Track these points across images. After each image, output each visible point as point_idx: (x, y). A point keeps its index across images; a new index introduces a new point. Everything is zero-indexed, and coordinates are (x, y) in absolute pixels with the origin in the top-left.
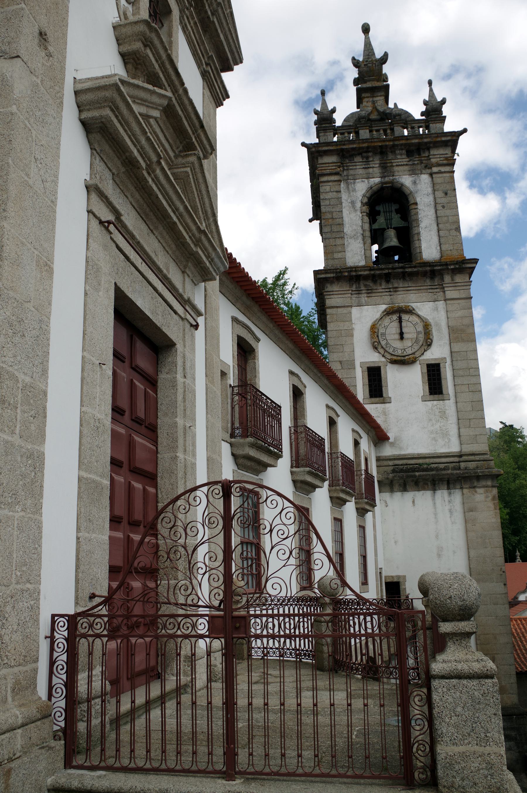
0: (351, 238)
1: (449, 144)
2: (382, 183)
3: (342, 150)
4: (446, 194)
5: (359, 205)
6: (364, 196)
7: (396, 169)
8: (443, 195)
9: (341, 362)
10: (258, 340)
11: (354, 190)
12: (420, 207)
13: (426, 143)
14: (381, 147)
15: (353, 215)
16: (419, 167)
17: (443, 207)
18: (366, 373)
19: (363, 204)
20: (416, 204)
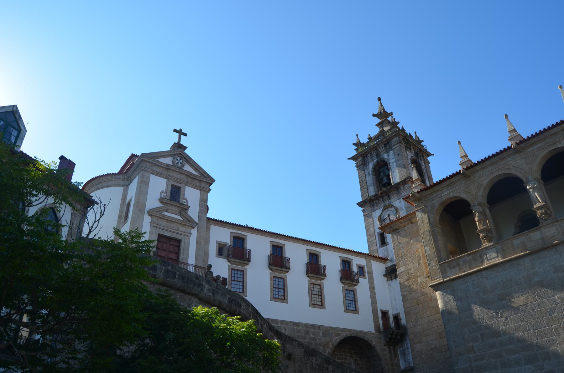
0: (369, 186)
1: (397, 135)
2: (377, 161)
3: (362, 155)
4: (399, 155)
5: (371, 172)
6: (372, 168)
7: (382, 153)
8: (398, 156)
9: (370, 235)
10: (247, 236)
11: (369, 168)
12: (390, 164)
13: (389, 139)
14: (374, 147)
15: (369, 178)
16: (389, 149)
17: (398, 161)
18: (379, 236)
19: (372, 172)
20: (389, 164)
